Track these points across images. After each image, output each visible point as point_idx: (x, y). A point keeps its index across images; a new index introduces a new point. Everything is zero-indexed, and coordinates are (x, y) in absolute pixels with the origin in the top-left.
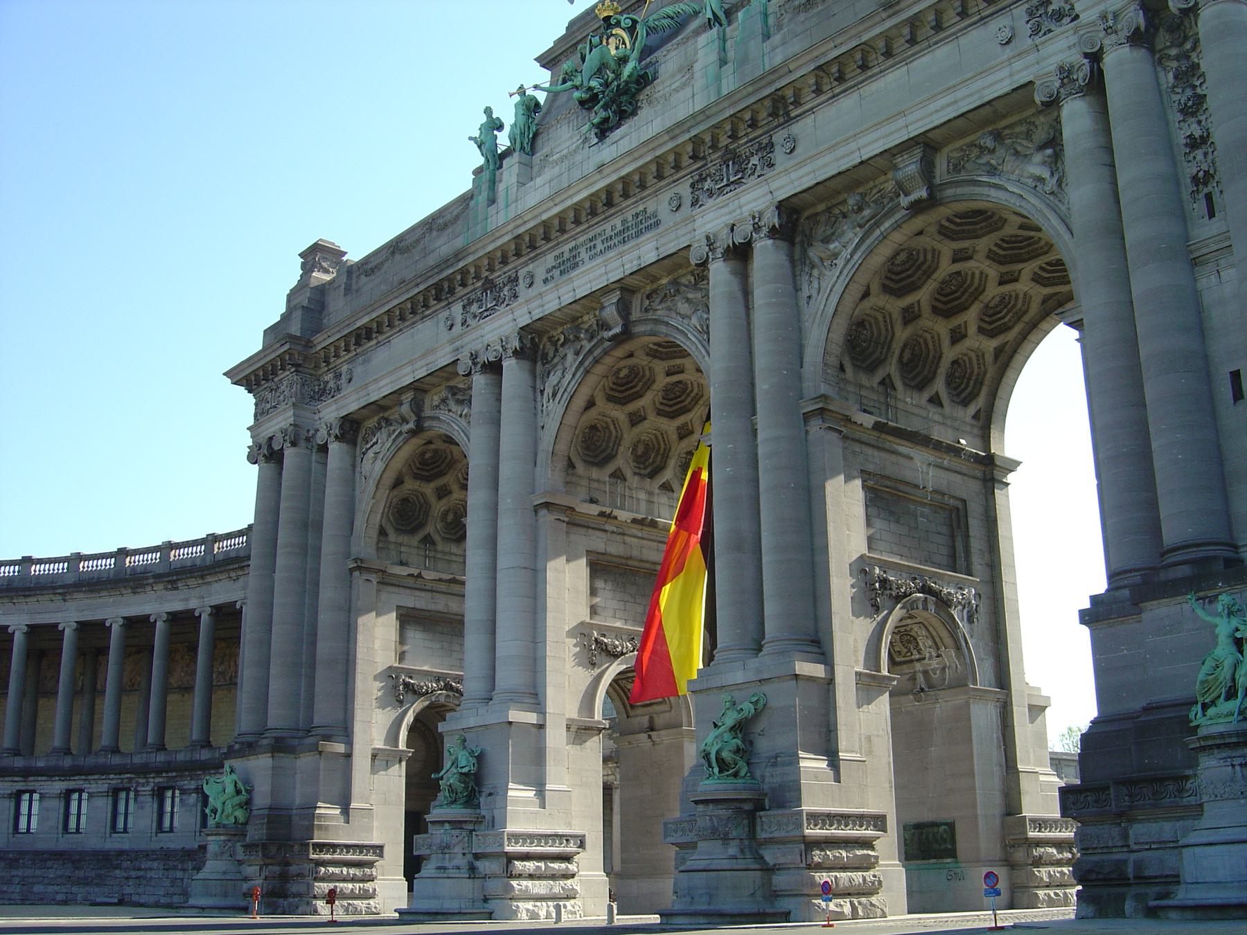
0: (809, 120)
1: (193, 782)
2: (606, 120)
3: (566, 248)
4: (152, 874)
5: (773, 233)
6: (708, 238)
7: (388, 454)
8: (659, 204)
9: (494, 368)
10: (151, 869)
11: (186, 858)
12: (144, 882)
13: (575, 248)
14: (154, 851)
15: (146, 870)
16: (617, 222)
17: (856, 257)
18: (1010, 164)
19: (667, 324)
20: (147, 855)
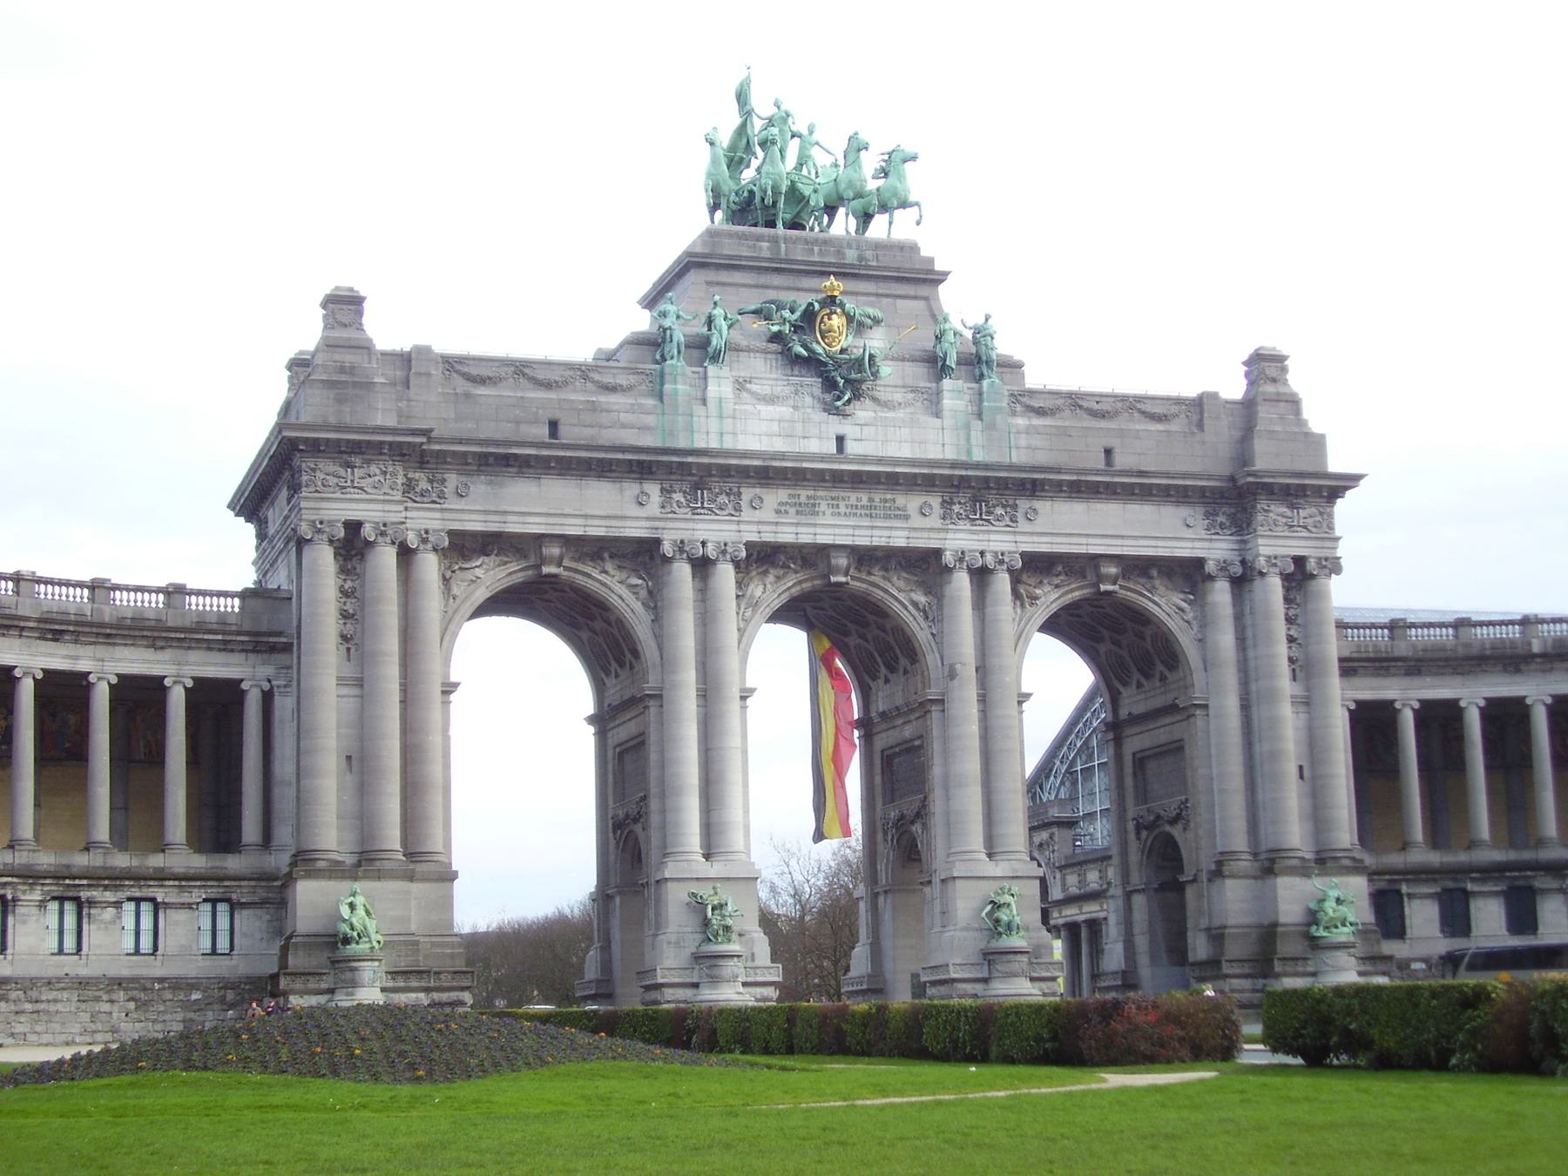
0: (1048, 504)
1: (107, 893)
2: (849, 401)
3: (804, 494)
4: (59, 1007)
5: (1011, 571)
6: (963, 553)
7: (497, 585)
8: (912, 502)
9: (703, 566)
10: (55, 1001)
11: (115, 987)
12: (43, 1017)
13: (814, 498)
14: (59, 980)
15: (49, 1001)
16: (865, 498)
17: (1053, 606)
18: (1162, 590)
19: (886, 591)
20: (49, 983)
